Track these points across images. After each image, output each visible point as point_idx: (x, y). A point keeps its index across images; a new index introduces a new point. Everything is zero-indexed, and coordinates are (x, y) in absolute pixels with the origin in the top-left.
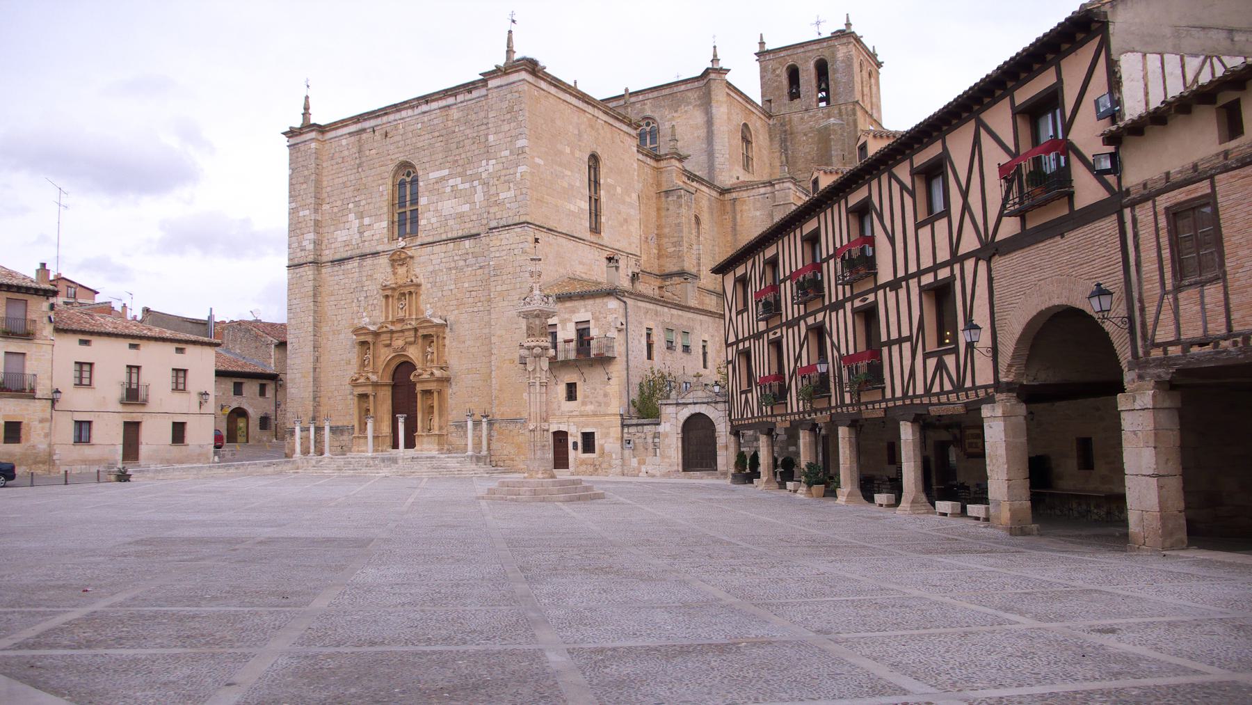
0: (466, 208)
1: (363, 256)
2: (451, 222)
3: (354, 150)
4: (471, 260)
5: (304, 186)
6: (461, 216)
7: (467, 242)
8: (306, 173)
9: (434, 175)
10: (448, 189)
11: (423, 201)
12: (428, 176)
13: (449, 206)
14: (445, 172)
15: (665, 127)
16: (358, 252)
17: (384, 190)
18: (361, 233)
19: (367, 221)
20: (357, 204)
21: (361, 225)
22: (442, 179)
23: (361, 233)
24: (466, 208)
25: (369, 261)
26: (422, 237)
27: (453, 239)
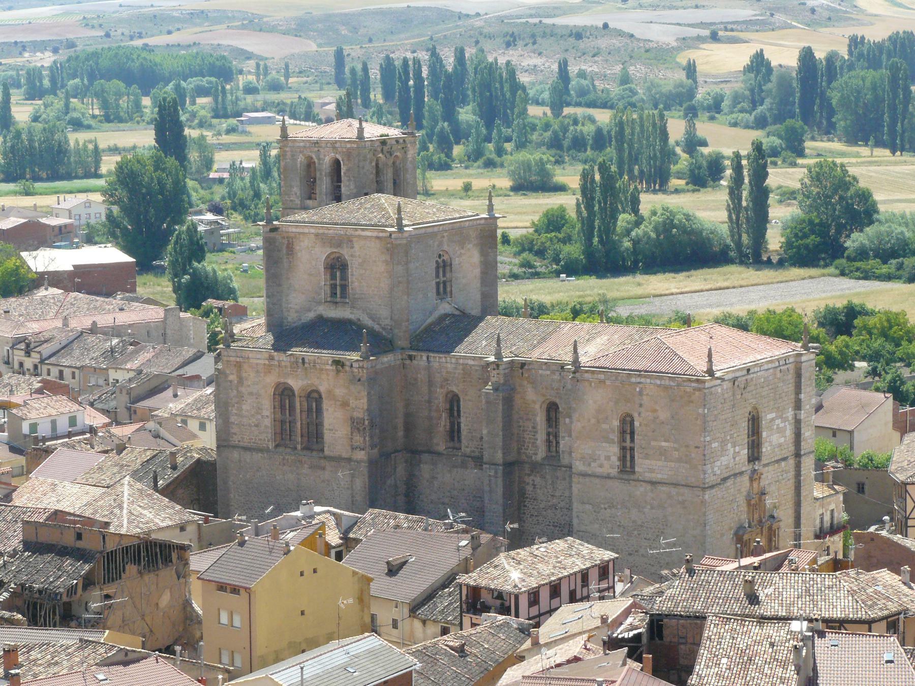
0: (782, 440)
1: (735, 475)
2: (776, 450)
3: (730, 394)
4: (785, 476)
5: (715, 423)
6: (780, 445)
7: (783, 464)
8: (716, 412)
9: (770, 416)
10: (775, 427)
11: (764, 434)
12: (768, 417)
13: (776, 439)
14: (774, 415)
15: (456, 262)
16: (732, 473)
17: (744, 425)
18: (734, 458)
19: (737, 449)
20: (732, 436)
21: (735, 452)
22: (773, 420)
23: (734, 458)
24: (782, 440)
25: (738, 479)
26: (764, 460)
27: (778, 461)
